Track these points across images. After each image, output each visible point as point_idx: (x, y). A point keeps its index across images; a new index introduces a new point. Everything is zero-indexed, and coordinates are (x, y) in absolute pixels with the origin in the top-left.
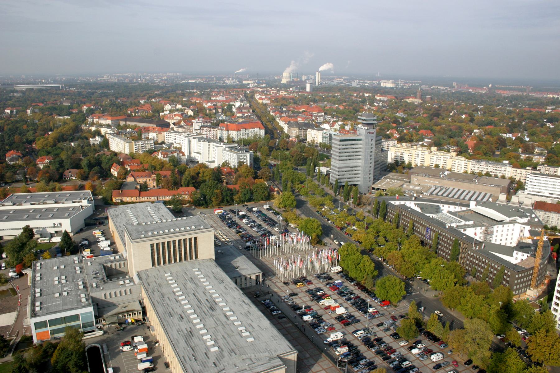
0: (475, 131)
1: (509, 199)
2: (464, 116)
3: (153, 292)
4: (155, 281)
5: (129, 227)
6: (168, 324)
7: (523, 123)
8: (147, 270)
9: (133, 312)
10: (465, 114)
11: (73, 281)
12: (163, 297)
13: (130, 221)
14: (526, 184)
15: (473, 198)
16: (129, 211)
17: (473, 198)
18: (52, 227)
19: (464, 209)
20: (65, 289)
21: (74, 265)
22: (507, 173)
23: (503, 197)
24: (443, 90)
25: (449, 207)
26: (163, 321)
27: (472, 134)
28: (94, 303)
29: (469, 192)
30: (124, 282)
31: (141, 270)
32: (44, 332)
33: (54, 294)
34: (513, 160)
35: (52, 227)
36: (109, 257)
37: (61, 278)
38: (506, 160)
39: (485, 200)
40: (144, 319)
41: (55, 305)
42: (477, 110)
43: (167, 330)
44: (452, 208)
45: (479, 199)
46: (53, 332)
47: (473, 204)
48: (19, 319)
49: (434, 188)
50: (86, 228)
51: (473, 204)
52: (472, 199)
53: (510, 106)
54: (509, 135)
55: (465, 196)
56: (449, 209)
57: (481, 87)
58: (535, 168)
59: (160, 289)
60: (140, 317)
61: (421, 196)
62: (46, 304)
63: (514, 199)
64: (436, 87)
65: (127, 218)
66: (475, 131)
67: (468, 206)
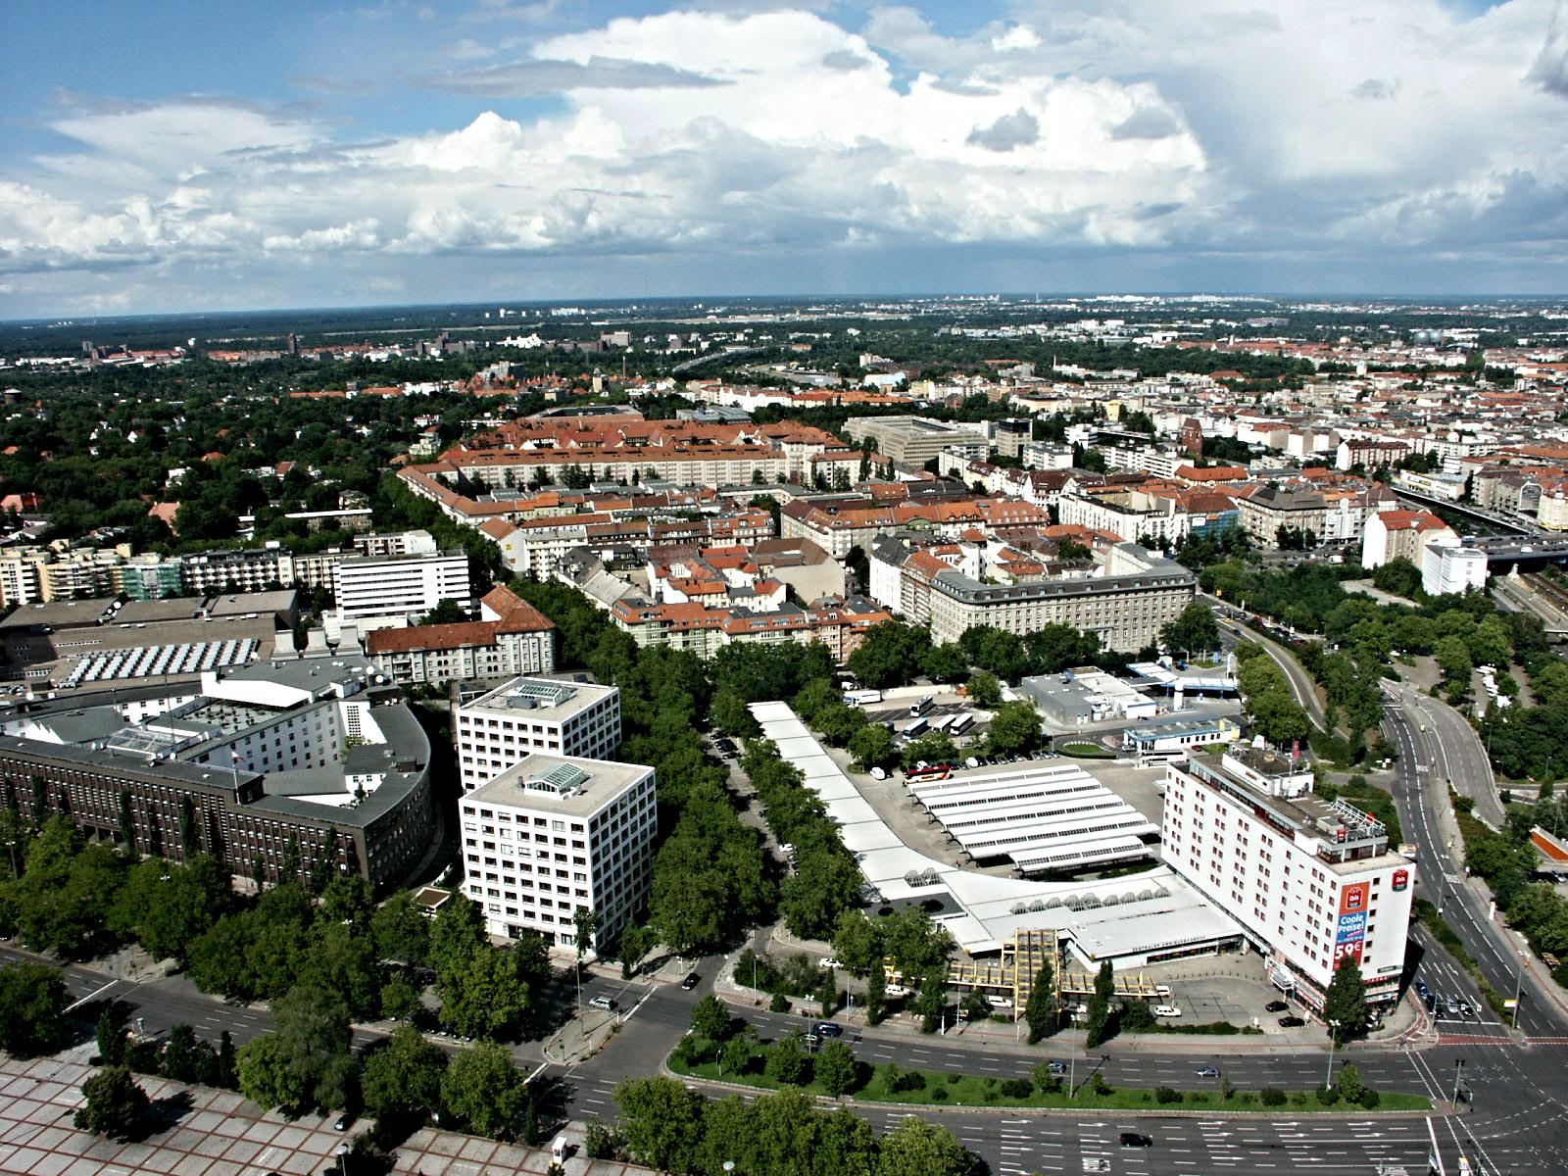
0: (172, 473)
1: (301, 642)
2: (132, 437)
7: (298, 434)
10: (137, 429)
14: (337, 593)
15: (207, 663)
17: (207, 663)
19: (188, 699)
22: (281, 573)
23: (284, 642)
24: (58, 367)
25: (143, 705)
27: (167, 483)
29: (191, 650)
34: (292, 537)
38: (272, 539)
39: (240, 659)
42: (169, 415)
44: (153, 708)
45: (224, 661)
47: (208, 680)
49: (88, 662)
51: (208, 680)
52: (203, 667)
53: (257, 393)
54: (267, 471)
55: (184, 663)
56: (144, 710)
57: (166, 346)
58: (347, 544)
61: (51, 695)
63: (315, 640)
64: (33, 361)
66: (172, 473)
67: (195, 687)
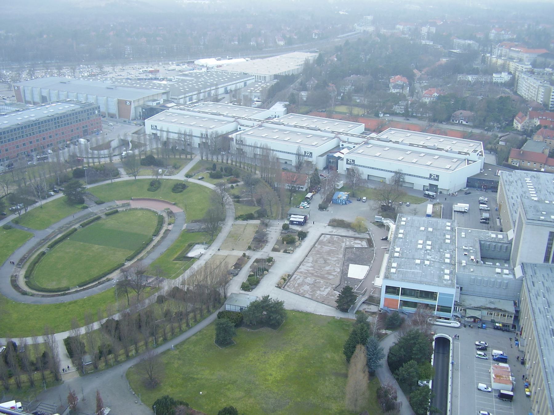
3: (537, 295)
4: (543, 282)
5: (526, 201)
6: (547, 344)
8: (535, 265)
9: (504, 313)
11: (439, 251)
12: (549, 307)
13: (527, 195)
16: (528, 180)
18: (427, 178)
20: (428, 257)
21: (444, 232)
26: (541, 337)
28: (458, 286)
30: (502, 271)
31: (528, 262)
32: (393, 300)
33: (414, 259)
35: (427, 178)
36: (490, 233)
37: (426, 243)
40: (514, 327)
41: (413, 273)
43: (544, 351)
46: (405, 303)
48: (371, 275)
50: (467, 189)
59: (546, 295)
60: (510, 321)
62: (403, 268)
65: (524, 190)
